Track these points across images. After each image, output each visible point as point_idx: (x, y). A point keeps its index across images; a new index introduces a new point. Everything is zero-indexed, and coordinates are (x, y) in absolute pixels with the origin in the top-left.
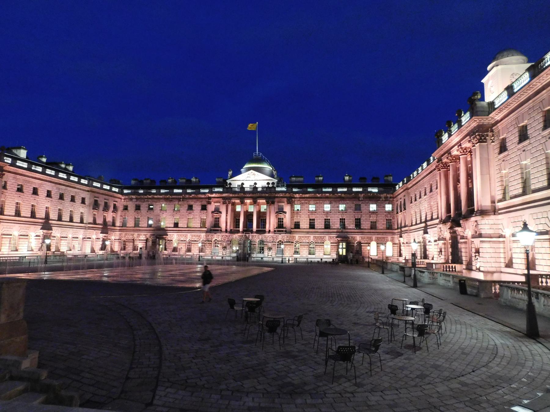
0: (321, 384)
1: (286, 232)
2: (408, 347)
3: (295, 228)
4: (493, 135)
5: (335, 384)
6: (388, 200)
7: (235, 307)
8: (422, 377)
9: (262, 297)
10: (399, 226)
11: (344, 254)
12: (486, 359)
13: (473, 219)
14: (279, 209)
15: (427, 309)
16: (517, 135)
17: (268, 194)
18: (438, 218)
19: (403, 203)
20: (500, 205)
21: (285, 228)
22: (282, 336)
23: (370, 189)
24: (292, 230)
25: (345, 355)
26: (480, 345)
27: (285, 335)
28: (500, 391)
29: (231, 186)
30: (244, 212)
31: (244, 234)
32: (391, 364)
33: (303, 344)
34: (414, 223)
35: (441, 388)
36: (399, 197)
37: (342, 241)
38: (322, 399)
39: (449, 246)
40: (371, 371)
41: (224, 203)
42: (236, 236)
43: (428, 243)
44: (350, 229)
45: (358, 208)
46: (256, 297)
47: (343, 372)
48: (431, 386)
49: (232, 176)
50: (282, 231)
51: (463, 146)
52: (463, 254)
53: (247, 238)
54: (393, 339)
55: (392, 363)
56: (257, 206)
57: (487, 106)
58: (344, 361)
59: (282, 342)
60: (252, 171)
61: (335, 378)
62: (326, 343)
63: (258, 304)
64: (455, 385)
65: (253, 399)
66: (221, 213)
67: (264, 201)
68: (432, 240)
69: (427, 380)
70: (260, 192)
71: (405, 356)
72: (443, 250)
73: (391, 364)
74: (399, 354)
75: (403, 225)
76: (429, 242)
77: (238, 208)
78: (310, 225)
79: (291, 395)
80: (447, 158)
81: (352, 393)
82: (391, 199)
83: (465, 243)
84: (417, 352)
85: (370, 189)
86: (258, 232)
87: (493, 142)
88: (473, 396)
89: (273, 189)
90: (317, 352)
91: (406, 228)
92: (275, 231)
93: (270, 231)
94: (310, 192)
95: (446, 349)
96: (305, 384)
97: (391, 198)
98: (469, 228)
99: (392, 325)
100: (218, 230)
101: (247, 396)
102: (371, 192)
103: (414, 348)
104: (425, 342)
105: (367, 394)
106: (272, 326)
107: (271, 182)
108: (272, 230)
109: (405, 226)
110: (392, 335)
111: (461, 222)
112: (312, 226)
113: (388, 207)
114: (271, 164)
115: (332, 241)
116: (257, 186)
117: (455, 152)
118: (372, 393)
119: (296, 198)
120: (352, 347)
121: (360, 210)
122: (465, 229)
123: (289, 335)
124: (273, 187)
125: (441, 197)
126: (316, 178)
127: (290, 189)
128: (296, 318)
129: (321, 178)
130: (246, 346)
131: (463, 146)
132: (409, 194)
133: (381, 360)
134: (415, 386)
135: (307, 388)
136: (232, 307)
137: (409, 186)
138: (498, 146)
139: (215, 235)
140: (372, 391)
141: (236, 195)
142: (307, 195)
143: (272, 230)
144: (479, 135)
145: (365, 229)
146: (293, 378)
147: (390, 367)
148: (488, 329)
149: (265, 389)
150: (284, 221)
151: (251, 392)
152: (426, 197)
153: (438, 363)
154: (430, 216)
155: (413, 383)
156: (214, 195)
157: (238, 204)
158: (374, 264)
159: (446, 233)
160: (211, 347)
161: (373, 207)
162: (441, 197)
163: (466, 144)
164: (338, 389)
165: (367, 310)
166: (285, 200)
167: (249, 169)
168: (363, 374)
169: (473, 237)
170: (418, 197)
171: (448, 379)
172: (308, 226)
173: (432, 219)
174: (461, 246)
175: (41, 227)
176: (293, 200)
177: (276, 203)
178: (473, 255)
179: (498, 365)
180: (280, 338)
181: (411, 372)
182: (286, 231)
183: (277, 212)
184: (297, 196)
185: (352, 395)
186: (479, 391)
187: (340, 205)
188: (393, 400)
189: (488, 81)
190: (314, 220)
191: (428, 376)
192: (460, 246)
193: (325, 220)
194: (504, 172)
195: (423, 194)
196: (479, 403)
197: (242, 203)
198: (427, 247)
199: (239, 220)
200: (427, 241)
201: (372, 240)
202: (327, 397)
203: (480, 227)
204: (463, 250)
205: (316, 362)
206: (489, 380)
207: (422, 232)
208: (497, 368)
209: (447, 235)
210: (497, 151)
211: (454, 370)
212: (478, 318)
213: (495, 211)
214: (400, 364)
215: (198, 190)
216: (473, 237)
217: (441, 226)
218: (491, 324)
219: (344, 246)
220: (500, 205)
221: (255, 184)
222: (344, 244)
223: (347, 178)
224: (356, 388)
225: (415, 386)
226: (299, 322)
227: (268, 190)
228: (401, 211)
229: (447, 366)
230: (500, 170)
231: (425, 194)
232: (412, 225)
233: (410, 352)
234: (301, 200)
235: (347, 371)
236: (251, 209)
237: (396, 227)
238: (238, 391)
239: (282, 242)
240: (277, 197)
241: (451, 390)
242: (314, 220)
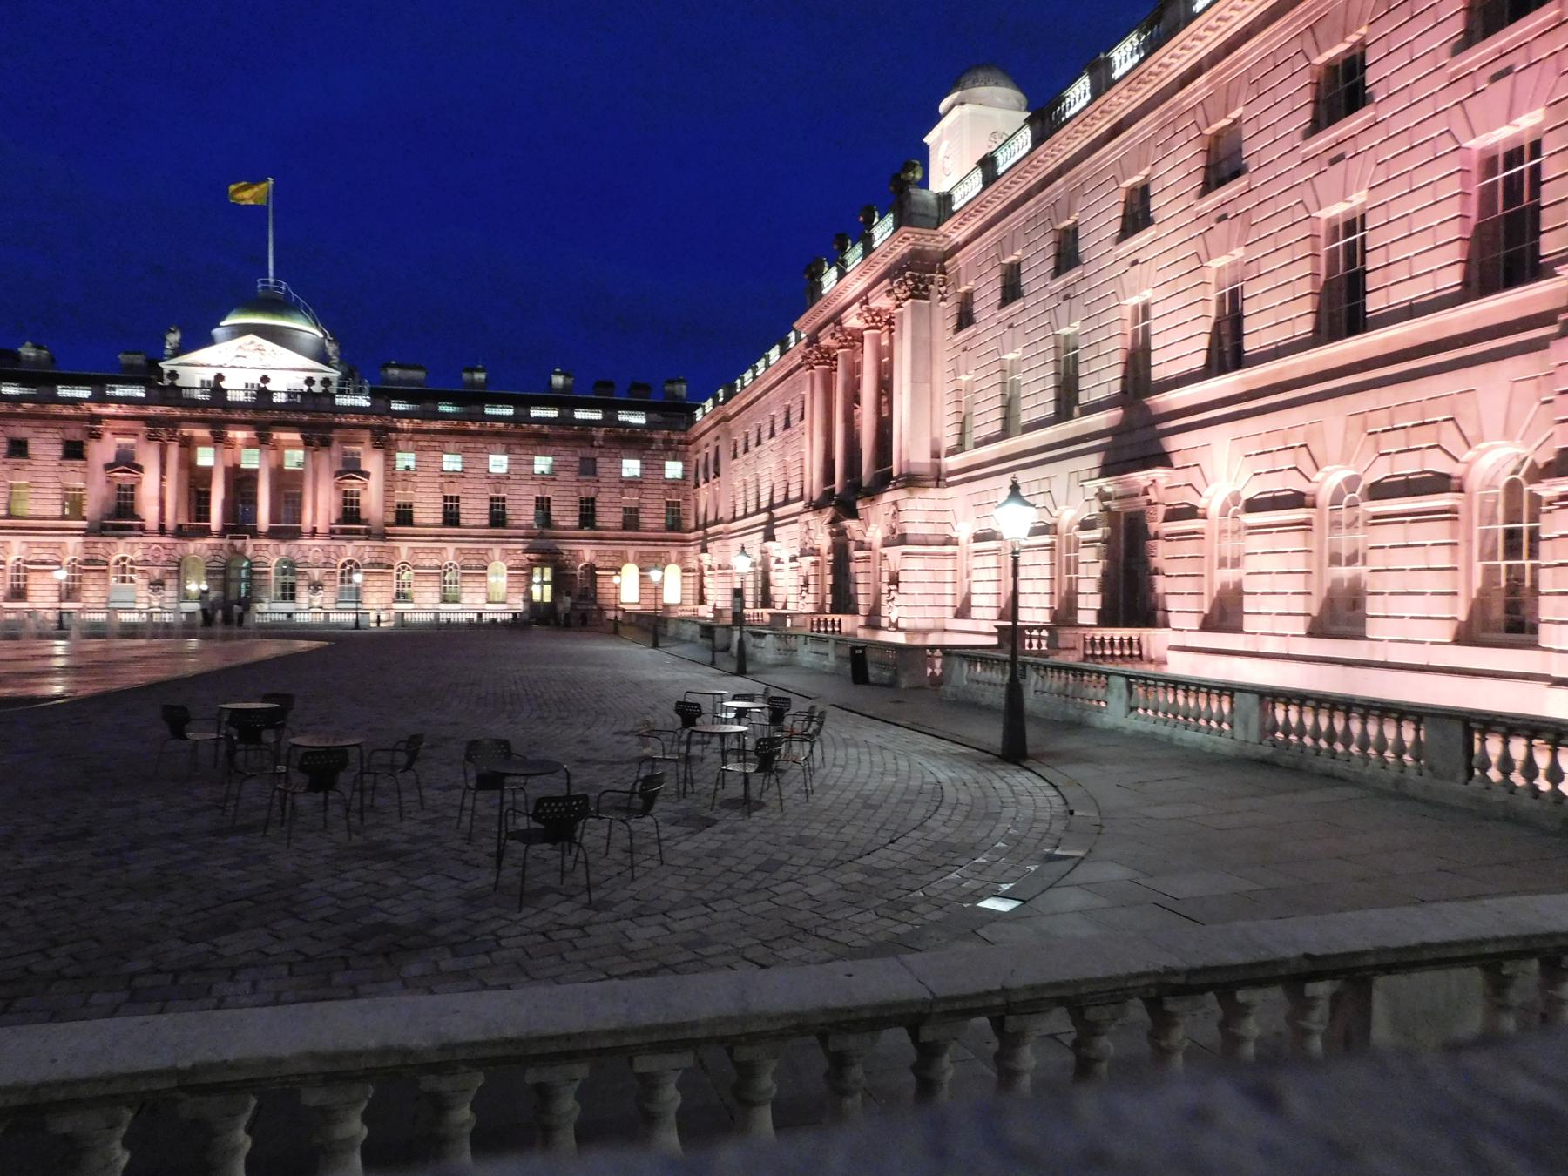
0: (484, 916)
1: (369, 535)
2: (731, 804)
3: (399, 523)
4: (945, 283)
5: (527, 911)
6: (674, 450)
7: (189, 735)
8: (770, 866)
9: (286, 700)
10: (701, 522)
11: (547, 599)
12: (918, 812)
13: (888, 497)
14: (345, 463)
15: (778, 709)
17: (311, 416)
18: (801, 498)
19: (711, 457)
20: (951, 463)
21: (365, 522)
22: (356, 805)
23: (623, 417)
25: (560, 821)
26: (903, 786)
27: (367, 802)
28: (954, 875)
29: (179, 383)
30: (227, 469)
31: (226, 541)
32: (686, 846)
33: (424, 822)
34: (740, 513)
35: (818, 888)
36: (703, 440)
37: (542, 563)
38: (488, 953)
39: (828, 570)
40: (632, 867)
41: (151, 438)
42: (197, 548)
43: (773, 566)
44: (565, 528)
45: (588, 469)
46: (266, 699)
47: (552, 879)
48: (792, 885)
49: (181, 350)
50: (357, 532)
51: (873, 305)
52: (861, 589)
53: (240, 554)
54: (689, 789)
55: (689, 845)
56: (272, 453)
57: (933, 202)
58: (553, 841)
59: (355, 820)
60: (251, 337)
61: (525, 897)
62: (496, 812)
63: (274, 720)
64: (851, 876)
65: (254, 984)
66: (139, 469)
67: (296, 436)
68: (785, 557)
69: (782, 873)
70: (279, 407)
71: (723, 826)
72: (812, 581)
73: (686, 846)
74: (710, 823)
75: (711, 518)
76: (778, 561)
77: (205, 457)
78: (445, 514)
79: (386, 955)
80: (833, 335)
81: (581, 928)
82: (682, 447)
83: (867, 559)
84: (755, 814)
85: (623, 417)
86: (274, 534)
87: (943, 300)
88: (895, 894)
89: (327, 400)
90: (470, 838)
91: (720, 527)
92: (332, 532)
93: (314, 533)
94: (445, 416)
95: (826, 802)
96: (434, 921)
97: (680, 442)
99: (688, 759)
100: (130, 528)
101: (231, 979)
102: (626, 424)
103: (747, 804)
104: (774, 789)
105: (622, 924)
106: (323, 770)
107: (318, 377)
108: (322, 526)
109: (717, 522)
110: (688, 780)
111: (859, 505)
112: (451, 517)
113: (673, 469)
114: (320, 319)
115: (511, 563)
116: (270, 387)
117: (853, 321)
118: (640, 920)
119: (403, 431)
120: (577, 798)
121: (594, 473)
122: (867, 525)
123: (380, 801)
124: (326, 394)
126: (466, 376)
127: (382, 402)
128: (402, 746)
129: (480, 376)
130: (230, 840)
131: (873, 305)
132: (729, 432)
133: (659, 841)
134: (755, 890)
135: (440, 930)
136: (178, 732)
137: (731, 412)
140: (638, 915)
141: (197, 414)
142: (438, 425)
143: (322, 526)
144: (912, 277)
145: (607, 529)
146: (394, 910)
147: (684, 854)
148: (921, 753)
149: (298, 952)
150: (363, 500)
151: (247, 966)
152: (773, 440)
153: (807, 832)
154: (783, 492)
155: (748, 885)
156: (112, 409)
157: (204, 443)
158: (630, 624)
160: (95, 855)
161: (631, 467)
164: (537, 923)
165: (616, 728)
166: (366, 435)
168: (610, 878)
169: (887, 543)
170: (753, 441)
171: (836, 864)
172: (439, 518)
173: (787, 501)
174: (857, 568)
176: (393, 436)
177: (335, 445)
178: (885, 589)
179: (944, 823)
180: (348, 810)
181: (741, 861)
184: (405, 424)
185: (577, 933)
186: (906, 881)
187: (537, 459)
188: (696, 931)
189: (940, 140)
191: (782, 863)
192: (855, 567)
193: (492, 499)
194: (964, 378)
195: (766, 433)
196: (908, 907)
197: (219, 439)
198: (773, 575)
199: (208, 494)
200: (773, 560)
201: (627, 561)
202: (504, 948)
203: (903, 516)
204: (861, 578)
205: (466, 863)
206: (927, 857)
207: (761, 535)
208: (943, 829)
209: (823, 540)
210: (952, 323)
211: (847, 844)
212: (894, 730)
213: (938, 478)
214: (712, 845)
215: (45, 390)
216: (887, 543)
217: (809, 517)
218: (926, 742)
219: (547, 578)
220: (951, 463)
221: (265, 379)
222: (548, 571)
223: (558, 380)
224: (591, 913)
225: (755, 890)
226: (413, 757)
227: (310, 401)
228: (707, 480)
229: (831, 836)
230: (956, 372)
231: (772, 435)
232: (734, 519)
233: (736, 814)
234: (417, 437)
235: (563, 874)
236: (251, 460)
237: (693, 525)
238: (198, 969)
239: (357, 566)
240: (340, 426)
241: (843, 887)
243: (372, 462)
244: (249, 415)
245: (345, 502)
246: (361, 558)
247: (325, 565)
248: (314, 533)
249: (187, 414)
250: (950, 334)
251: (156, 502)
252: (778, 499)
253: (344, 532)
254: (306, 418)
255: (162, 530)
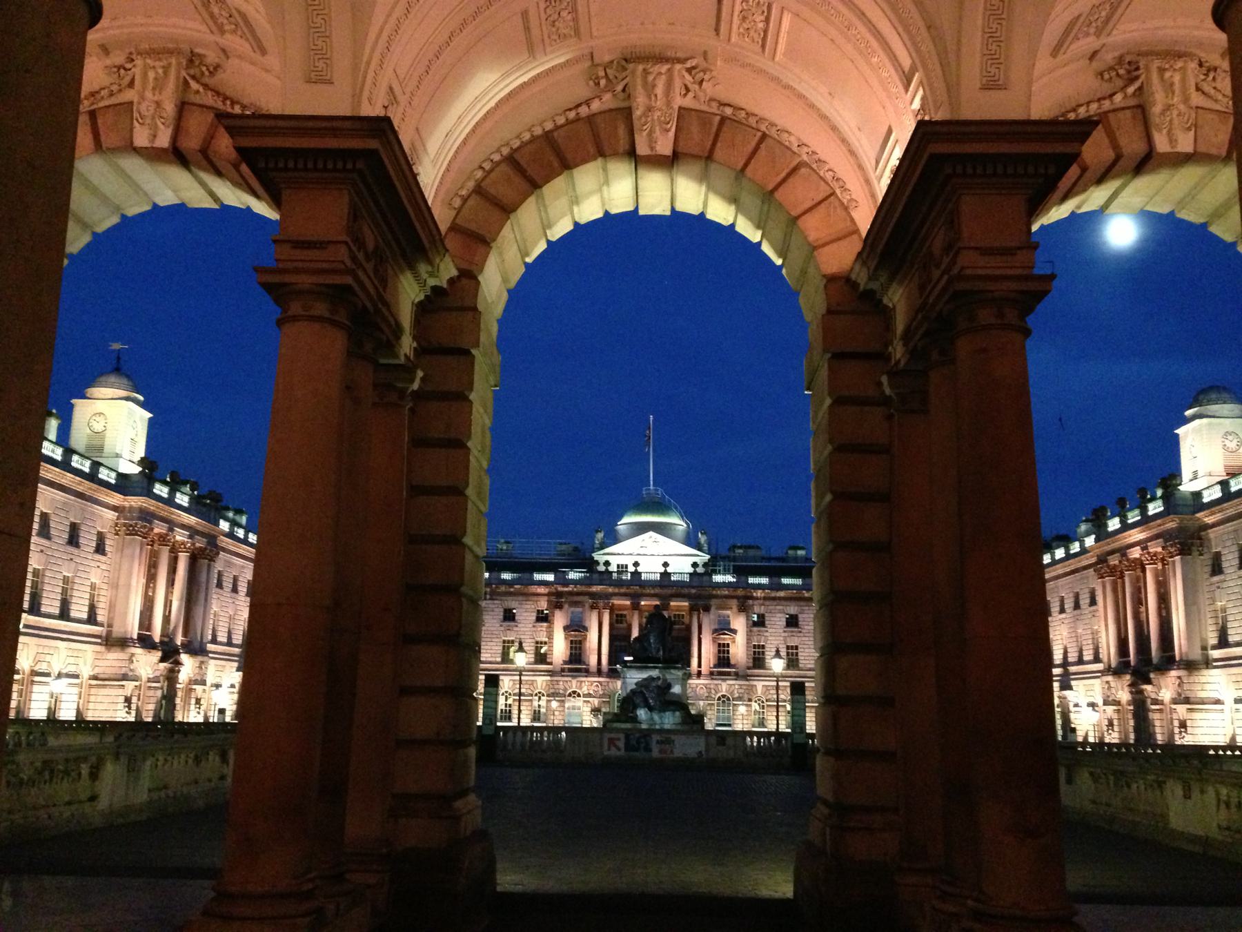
1: (737, 676)
13: (1174, 673)
14: (720, 622)
16: (1237, 555)
18: (1097, 659)
20: (1216, 654)
24: (749, 672)
39: (1130, 716)
41: (592, 608)
43: (1072, 708)
50: (728, 674)
52: (1158, 730)
68: (1083, 702)
72: (1115, 722)
76: (1076, 705)
83: (1160, 711)
89: (706, 578)
92: (712, 673)
93: (699, 674)
94: (787, 587)
98: (1167, 687)
111: (1152, 675)
114: (685, 515)
116: (669, 570)
119: (757, 598)
122: (1160, 688)
124: (706, 573)
125: (1106, 625)
138: (1210, 562)
139: (574, 682)
141: (623, 591)
142: (782, 594)
143: (704, 670)
152: (1063, 616)
154: (1076, 654)
159: (1120, 692)
162: (1106, 625)
163: (1156, 548)
166: (734, 603)
167: (641, 529)
169: (1175, 701)
173: (1080, 661)
174: (1155, 717)
175: (236, 664)
176: (750, 602)
177: (713, 609)
178: (1177, 730)
182: (737, 674)
183: (715, 631)
184: (759, 593)
189: (1186, 433)
190: (797, 648)
192: (1151, 715)
198: (1072, 716)
200: (1071, 705)
203: (1186, 687)
204: (1157, 723)
209: (1124, 696)
210: (1208, 569)
215: (527, 575)
216: (1175, 701)
217: (1110, 678)
221: (666, 565)
227: (696, 579)
231: (1062, 611)
239: (728, 699)
240: (716, 597)
242: (797, 648)
243: (739, 623)
244: (657, 591)
245: (719, 651)
246: (732, 693)
247: (707, 698)
248: (699, 674)
249: (616, 590)
250: (1206, 576)
251: (596, 652)
252: (1072, 657)
253: (720, 674)
254: (693, 591)
255: (599, 672)
